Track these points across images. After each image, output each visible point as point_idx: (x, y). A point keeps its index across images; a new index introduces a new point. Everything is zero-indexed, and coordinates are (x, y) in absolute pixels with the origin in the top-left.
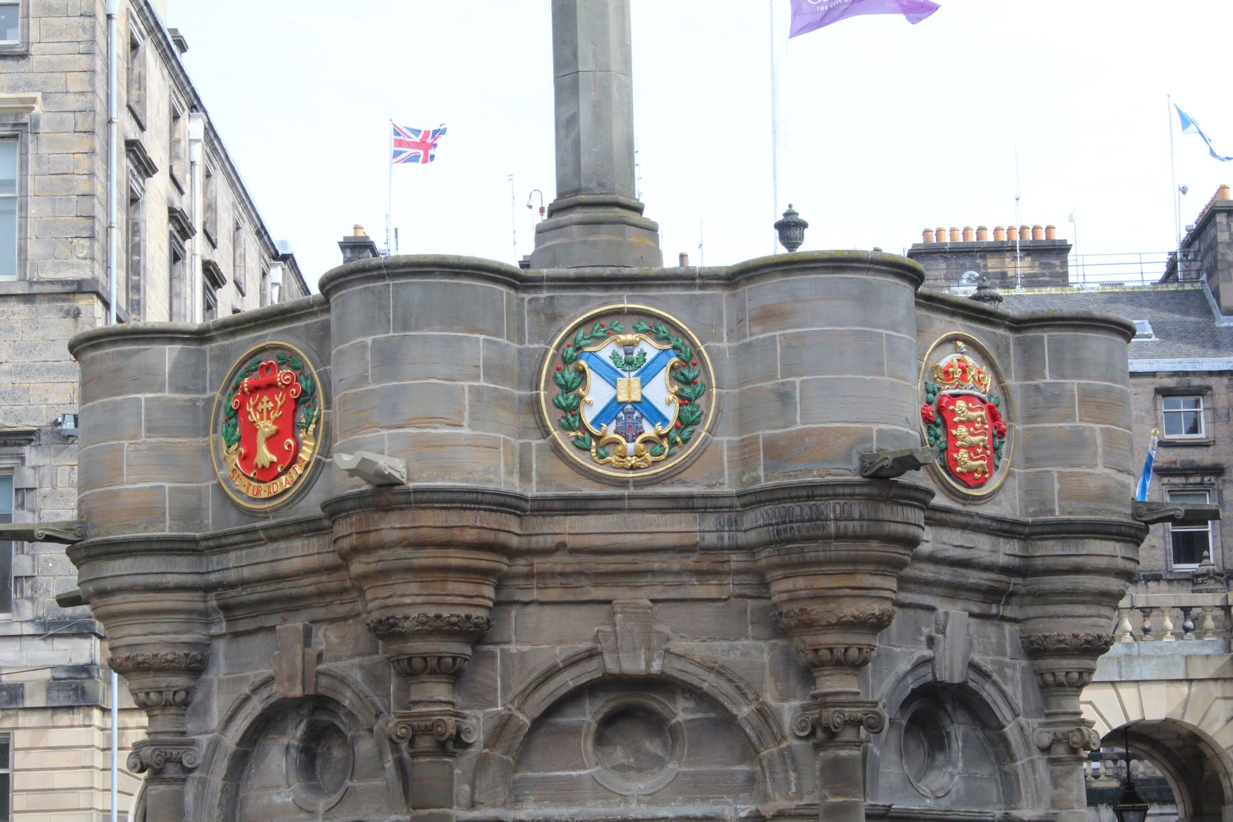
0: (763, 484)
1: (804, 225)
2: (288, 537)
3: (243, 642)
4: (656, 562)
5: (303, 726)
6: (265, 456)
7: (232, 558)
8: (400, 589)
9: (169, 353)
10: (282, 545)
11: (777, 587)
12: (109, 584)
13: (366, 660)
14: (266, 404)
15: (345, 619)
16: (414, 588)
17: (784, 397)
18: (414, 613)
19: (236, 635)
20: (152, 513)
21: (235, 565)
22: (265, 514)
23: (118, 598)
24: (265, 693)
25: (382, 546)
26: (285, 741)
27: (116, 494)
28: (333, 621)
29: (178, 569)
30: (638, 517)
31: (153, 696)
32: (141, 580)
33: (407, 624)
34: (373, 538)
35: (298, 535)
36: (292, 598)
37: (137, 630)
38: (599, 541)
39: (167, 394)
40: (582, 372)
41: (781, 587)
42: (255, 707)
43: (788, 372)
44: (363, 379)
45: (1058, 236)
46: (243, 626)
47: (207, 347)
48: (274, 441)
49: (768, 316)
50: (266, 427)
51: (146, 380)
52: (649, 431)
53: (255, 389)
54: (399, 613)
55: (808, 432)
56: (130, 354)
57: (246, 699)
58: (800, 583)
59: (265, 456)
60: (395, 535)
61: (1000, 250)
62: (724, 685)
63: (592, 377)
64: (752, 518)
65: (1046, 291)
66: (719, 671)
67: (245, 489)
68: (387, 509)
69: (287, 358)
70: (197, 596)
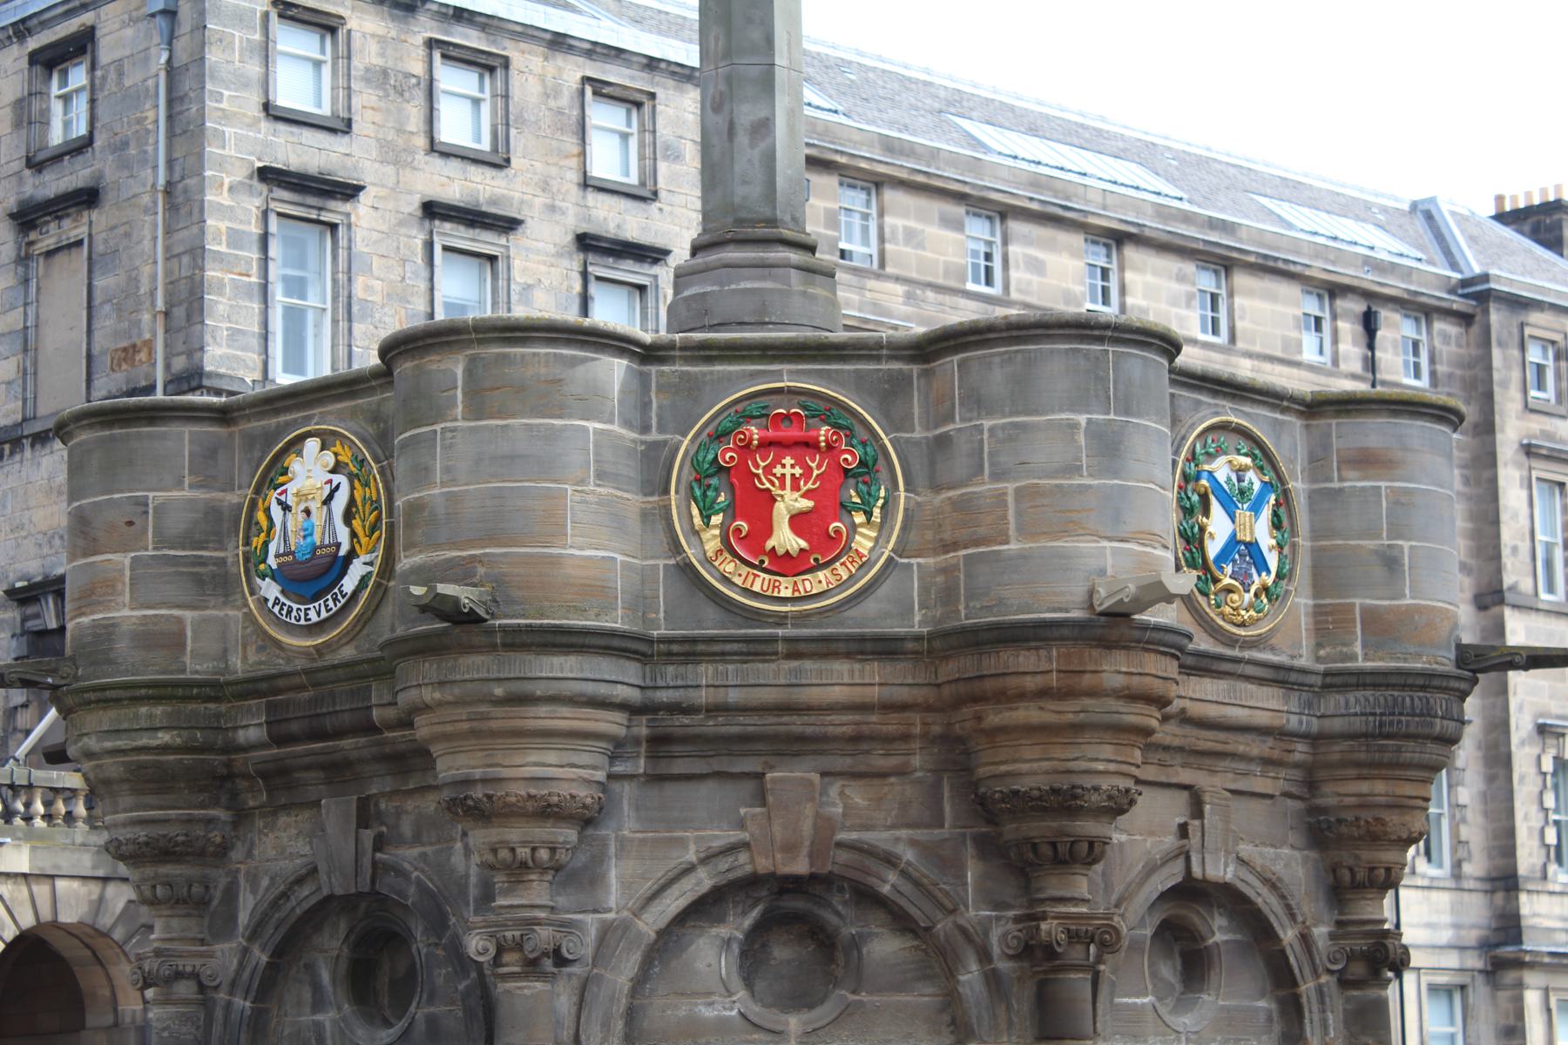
0: (1360, 664)
3: (671, 789)
4: (1241, 744)
5: (755, 913)
6: (785, 539)
7: (705, 673)
8: (1091, 751)
9: (615, 370)
10: (808, 664)
11: (1328, 789)
12: (539, 689)
13: (921, 834)
14: (788, 467)
15: (882, 775)
16: (1107, 751)
17: (1391, 562)
19: (656, 779)
20: (599, 592)
21: (705, 682)
22: (781, 620)
23: (543, 710)
24: (724, 864)
25: (1094, 693)
26: (723, 931)
27: (555, 561)
29: (620, 678)
30: (1242, 686)
31: (543, 854)
32: (590, 688)
33: (1095, 797)
34: (1087, 680)
35: (848, 655)
36: (802, 738)
37: (552, 757)
38: (1212, 712)
39: (615, 428)
40: (1205, 499)
42: (703, 881)
43: (1395, 532)
44: (1073, 469)
46: (679, 767)
47: (653, 369)
48: (798, 522)
49: (1366, 461)
51: (590, 405)
53: (766, 444)
54: (1088, 782)
55: (1418, 609)
56: (574, 362)
57: (689, 869)
58: (1380, 787)
60: (1118, 681)
62: (1274, 901)
63: (1215, 506)
66: (1273, 884)
67: (742, 580)
68: (1108, 645)
69: (829, 410)
70: (620, 717)
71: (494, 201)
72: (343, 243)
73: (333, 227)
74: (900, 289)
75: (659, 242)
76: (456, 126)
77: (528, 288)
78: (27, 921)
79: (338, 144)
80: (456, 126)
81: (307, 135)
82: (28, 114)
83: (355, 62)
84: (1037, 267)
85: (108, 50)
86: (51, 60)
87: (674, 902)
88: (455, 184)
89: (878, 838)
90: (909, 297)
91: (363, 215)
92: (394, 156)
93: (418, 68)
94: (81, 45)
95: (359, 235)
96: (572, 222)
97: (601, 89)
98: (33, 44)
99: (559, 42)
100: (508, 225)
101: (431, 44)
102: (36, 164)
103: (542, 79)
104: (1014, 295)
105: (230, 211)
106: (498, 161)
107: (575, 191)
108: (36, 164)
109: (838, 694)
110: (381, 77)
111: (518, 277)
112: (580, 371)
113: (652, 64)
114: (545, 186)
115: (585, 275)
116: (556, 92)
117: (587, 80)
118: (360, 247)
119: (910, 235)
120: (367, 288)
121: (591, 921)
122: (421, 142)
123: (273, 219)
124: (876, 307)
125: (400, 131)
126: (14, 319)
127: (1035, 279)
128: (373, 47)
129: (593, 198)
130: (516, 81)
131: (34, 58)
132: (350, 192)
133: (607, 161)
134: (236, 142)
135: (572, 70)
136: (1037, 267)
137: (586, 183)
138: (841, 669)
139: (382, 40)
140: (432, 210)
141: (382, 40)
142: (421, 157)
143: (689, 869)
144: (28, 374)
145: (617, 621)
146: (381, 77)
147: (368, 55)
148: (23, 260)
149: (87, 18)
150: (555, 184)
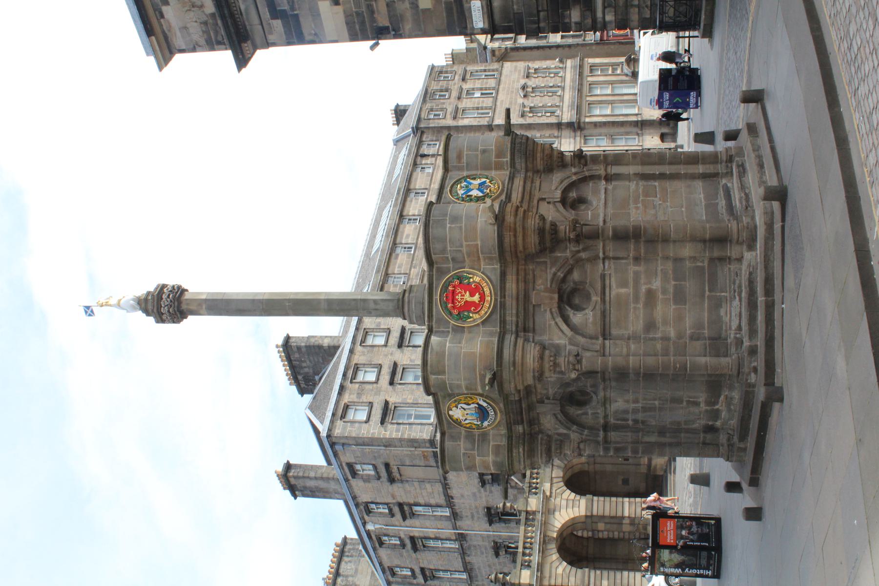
0: (509, 159)
2: (505, 287)
3: (537, 327)
4: (528, 188)
5: (567, 307)
7: (508, 318)
9: (434, 339)
11: (539, 167)
12: (512, 359)
13: (549, 266)
14: (459, 297)
16: (529, 221)
17: (484, 151)
18: (537, 221)
19: (534, 330)
21: (511, 318)
22: (496, 300)
23: (517, 358)
24: (555, 315)
25: (515, 224)
26: (571, 315)
27: (480, 354)
28: (534, 282)
29: (510, 339)
31: (552, 359)
32: (512, 347)
34: (512, 225)
35: (505, 283)
36: (525, 295)
37: (528, 356)
38: (520, 195)
40: (468, 196)
41: (540, 167)
42: (559, 320)
43: (477, 150)
44: (461, 228)
47: (434, 330)
48: (472, 295)
49: (459, 157)
50: (467, 297)
53: (453, 302)
54: (537, 226)
56: (432, 349)
57: (556, 323)
58: (538, 155)
59: (476, 298)
60: (512, 218)
64: (518, 166)
66: (562, 182)
68: (503, 220)
70: (519, 339)
73: (395, 407)
75: (400, 328)
76: (371, 377)
77: (411, 360)
78: (562, 484)
79: (375, 405)
80: (371, 377)
81: (373, 412)
82: (367, 479)
83: (356, 400)
85: (352, 460)
86: (354, 473)
87: (564, 327)
89: (549, 277)
91: (392, 400)
92: (378, 392)
93: (357, 385)
94: (350, 466)
95: (397, 401)
96: (395, 349)
97: (363, 341)
98: (350, 477)
99: (352, 351)
100: (395, 365)
102: (379, 478)
105: (391, 432)
106: (380, 367)
107: (387, 348)
108: (379, 478)
109: (514, 286)
110: (359, 395)
111: (408, 362)
112: (434, 347)
113: (357, 329)
114: (386, 355)
116: (363, 352)
118: (400, 401)
119: (400, 267)
121: (568, 347)
122: (375, 385)
126: (416, 484)
128: (352, 396)
129: (389, 344)
131: (353, 477)
133: (380, 341)
134: (374, 430)
135: (358, 348)
136: (408, 236)
137: (386, 345)
138: (508, 285)
139: (350, 394)
140: (392, 383)
141: (350, 394)
143: (556, 323)
144: (430, 481)
145: (495, 340)
146: (359, 395)
147: (354, 398)
148: (402, 481)
149: (344, 464)
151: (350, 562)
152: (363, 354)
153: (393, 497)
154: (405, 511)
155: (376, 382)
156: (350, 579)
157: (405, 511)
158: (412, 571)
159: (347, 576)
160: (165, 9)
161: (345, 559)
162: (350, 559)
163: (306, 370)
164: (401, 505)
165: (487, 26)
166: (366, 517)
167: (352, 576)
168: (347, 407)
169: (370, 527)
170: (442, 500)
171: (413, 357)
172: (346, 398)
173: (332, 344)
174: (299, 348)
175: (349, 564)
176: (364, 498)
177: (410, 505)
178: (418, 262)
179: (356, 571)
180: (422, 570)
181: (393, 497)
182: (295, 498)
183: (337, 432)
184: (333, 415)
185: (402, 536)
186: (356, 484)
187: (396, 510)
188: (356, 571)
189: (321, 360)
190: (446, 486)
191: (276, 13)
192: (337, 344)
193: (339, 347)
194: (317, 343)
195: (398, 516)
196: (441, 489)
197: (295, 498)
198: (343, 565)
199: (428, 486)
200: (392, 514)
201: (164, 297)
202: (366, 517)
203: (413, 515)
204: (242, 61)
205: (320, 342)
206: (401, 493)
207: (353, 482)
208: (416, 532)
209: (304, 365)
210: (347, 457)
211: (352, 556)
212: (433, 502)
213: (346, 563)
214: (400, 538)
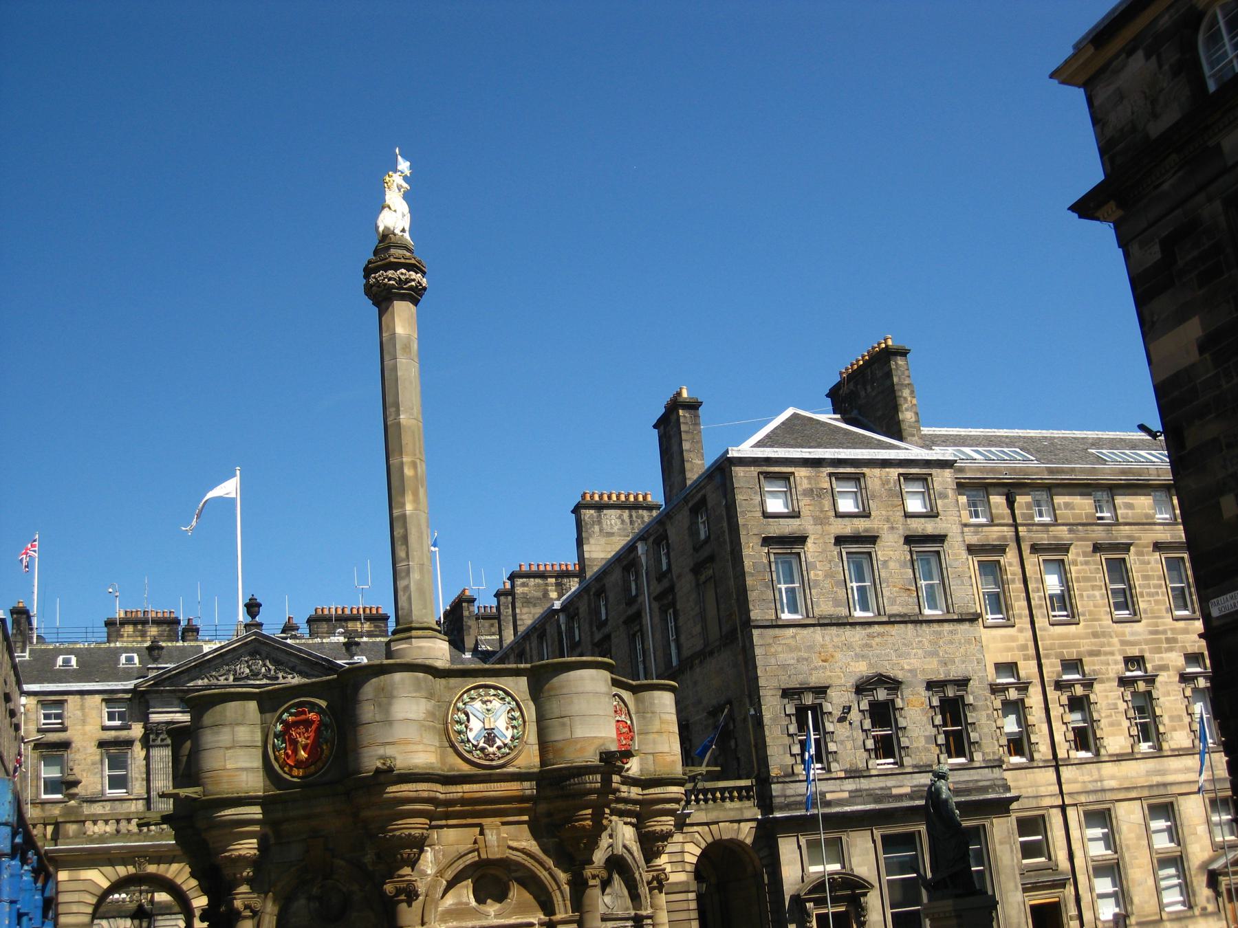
1: (259, 605)
45: (381, 611)
52: (499, 743)
61: (355, 618)
65: (378, 639)
71: (866, 530)
72: (803, 559)
74: (1065, 528)
75: (942, 533)
77: (885, 562)
78: (710, 840)
79: (796, 522)
80: (847, 505)
83: (799, 488)
84: (1130, 506)
86: (695, 511)
88: (846, 527)
90: (1070, 531)
91: (810, 549)
92: (820, 521)
93: (827, 485)
94: (703, 501)
95: (809, 555)
96: (901, 531)
97: (908, 478)
98: (690, 505)
99: (885, 463)
100: (873, 539)
101: (830, 475)
103: (880, 478)
104: (1121, 520)
105: (753, 554)
106: (865, 514)
107: (902, 519)
108: (696, 549)
110: (809, 493)
113: (928, 463)
114: (888, 520)
115: (911, 552)
116: (888, 482)
117: (899, 475)
118: (810, 559)
119: (1067, 505)
120: (816, 575)
123: (772, 557)
124: (1055, 537)
125: (822, 511)
127: (1130, 511)
128: (805, 481)
130: (869, 481)
131: (691, 510)
132: (802, 540)
133: (915, 505)
135: (894, 472)
136: (1130, 506)
137: (907, 515)
139: (809, 478)
141: (809, 478)
142: (832, 519)
144: (705, 628)
146: (809, 493)
148: (698, 585)
149: (703, 492)
150: (892, 519)
151: (623, 522)
152: (885, 483)
153: (679, 576)
154: (666, 599)
155: (839, 515)
156: (597, 528)
157: (666, 599)
158: (605, 623)
159: (600, 522)
160: (1140, 54)
161: (626, 514)
162: (627, 520)
163: (863, 393)
164: (671, 589)
165: (1215, 623)
166: (651, 539)
167: (601, 530)
168: (786, 477)
169: (641, 548)
170: (686, 653)
171: (892, 564)
172: (801, 473)
173: (904, 426)
174: (889, 375)
175: (619, 522)
176: (672, 532)
177: (673, 604)
178: (1082, 535)
179: (610, 534)
180: (608, 637)
181: (679, 576)
182: (655, 427)
183: (739, 472)
184: (768, 461)
185: (640, 599)
186: (683, 518)
187: (666, 583)
188: (610, 534)
189: (879, 413)
190: (704, 655)
191: (1168, 245)
192: (904, 434)
193: (901, 439)
194: (901, 401)
195: (658, 589)
196: (698, 649)
197: (655, 427)
198: (619, 512)
199: (698, 628)
200: (661, 576)
201: (390, 273)
202: (651, 539)
203: (663, 611)
204: (1086, 208)
205: (905, 406)
206: (685, 585)
207: (685, 512)
208: (647, 619)
209: (869, 388)
210: (713, 498)
211: (632, 522)
212: (683, 638)
213: (620, 517)
214: (637, 596)
